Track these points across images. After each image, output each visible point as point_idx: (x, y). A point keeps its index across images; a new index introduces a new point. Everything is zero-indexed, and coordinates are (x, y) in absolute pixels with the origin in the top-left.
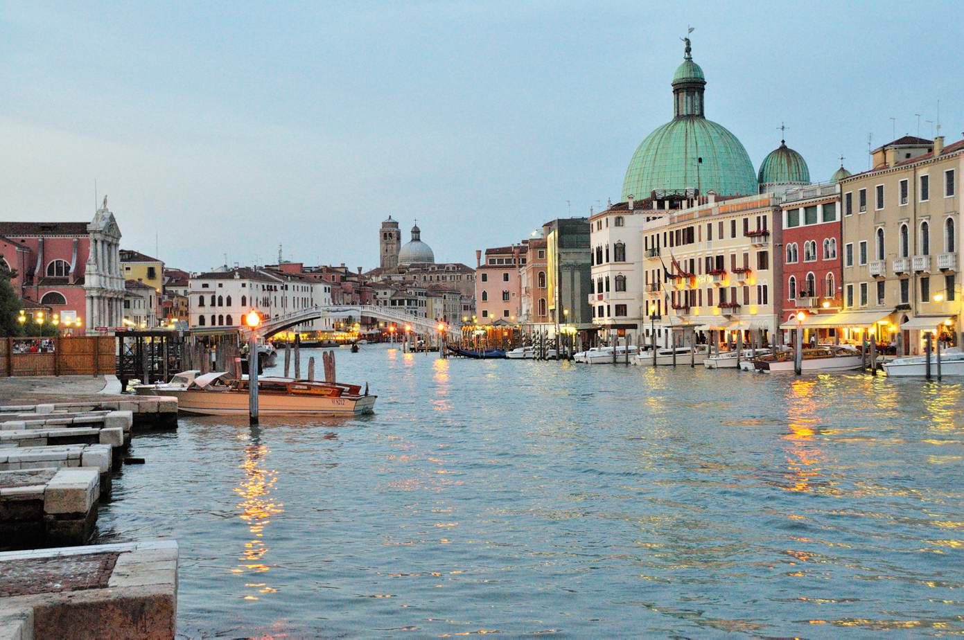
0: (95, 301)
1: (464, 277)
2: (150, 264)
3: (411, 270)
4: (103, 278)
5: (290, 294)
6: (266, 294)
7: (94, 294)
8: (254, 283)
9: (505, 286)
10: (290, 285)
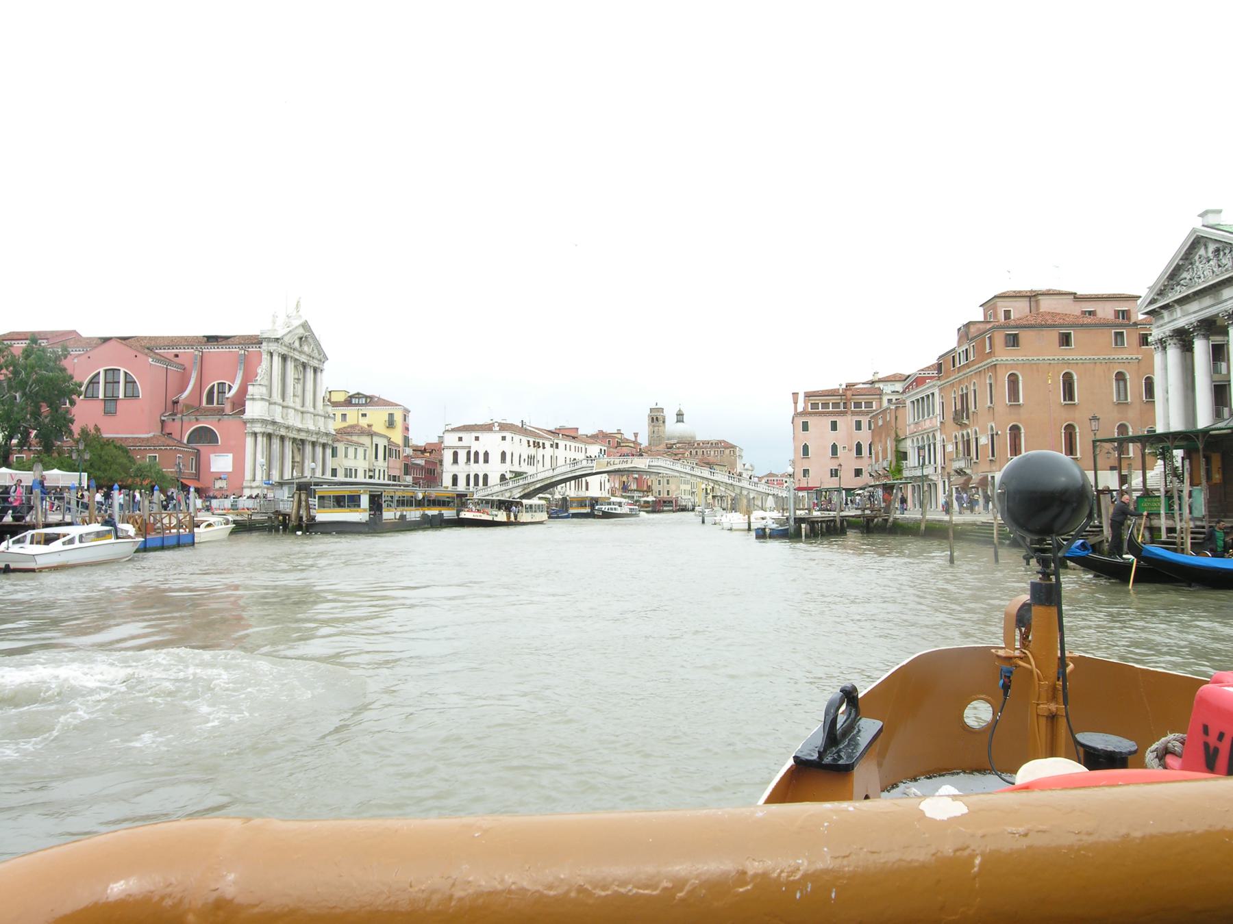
0: (260, 438)
1: (727, 451)
2: (390, 410)
4: (279, 409)
5: (561, 453)
6: (532, 451)
7: (258, 428)
8: (524, 440)
10: (562, 444)
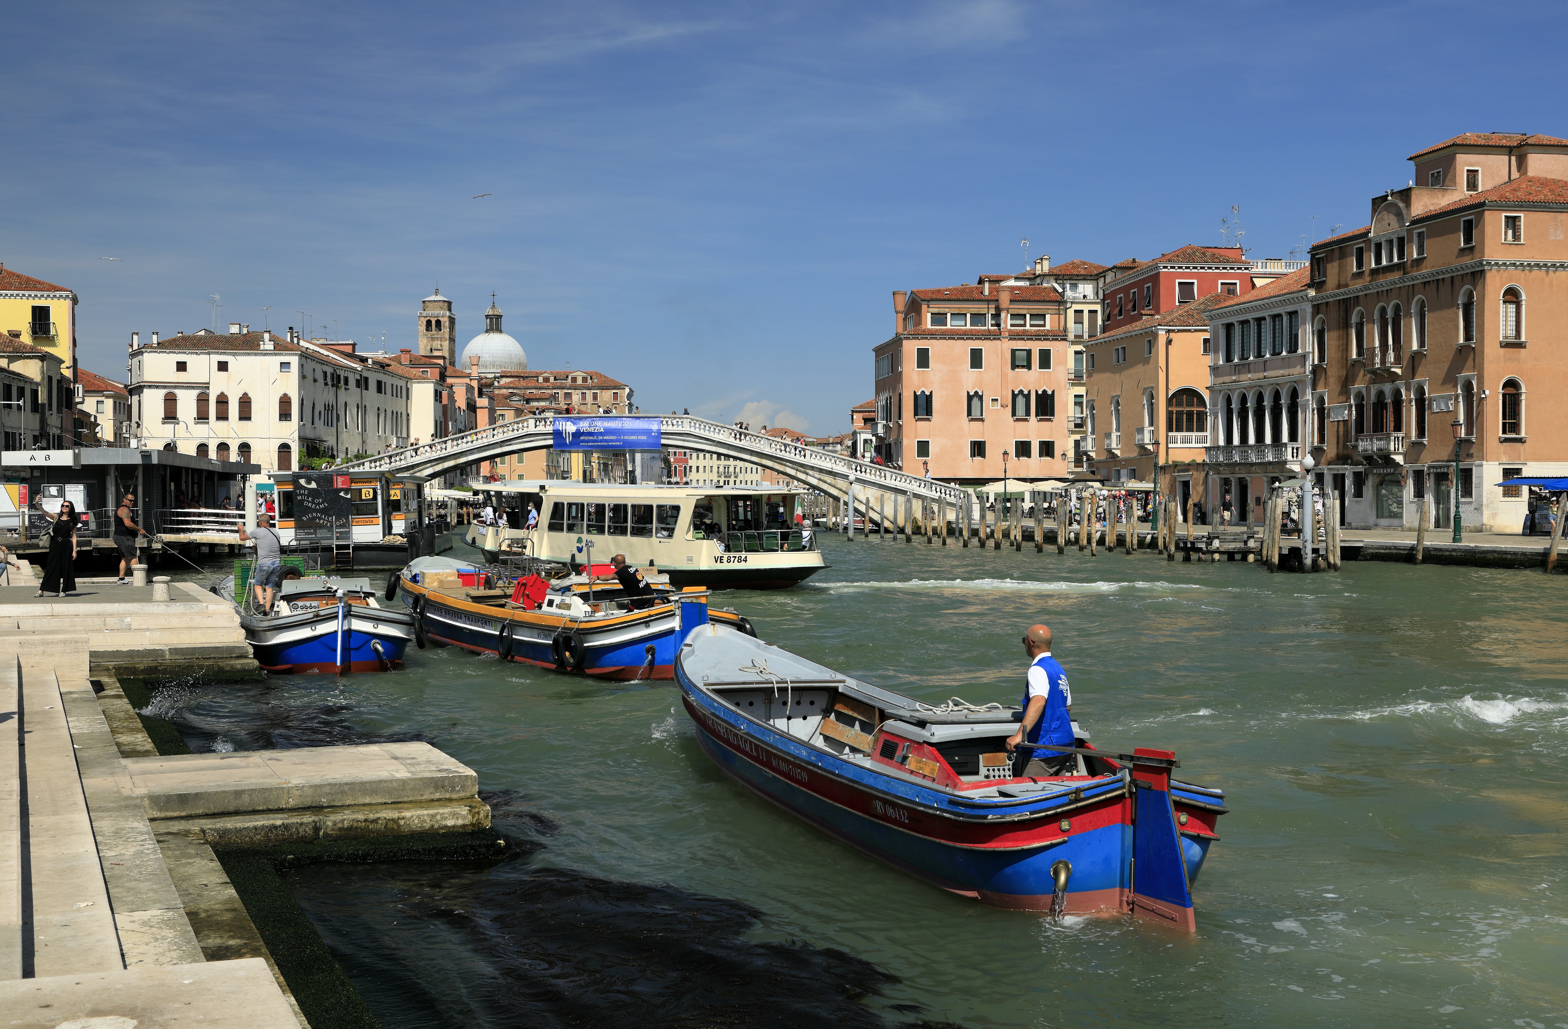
3: (503, 381)
9: (971, 380)
